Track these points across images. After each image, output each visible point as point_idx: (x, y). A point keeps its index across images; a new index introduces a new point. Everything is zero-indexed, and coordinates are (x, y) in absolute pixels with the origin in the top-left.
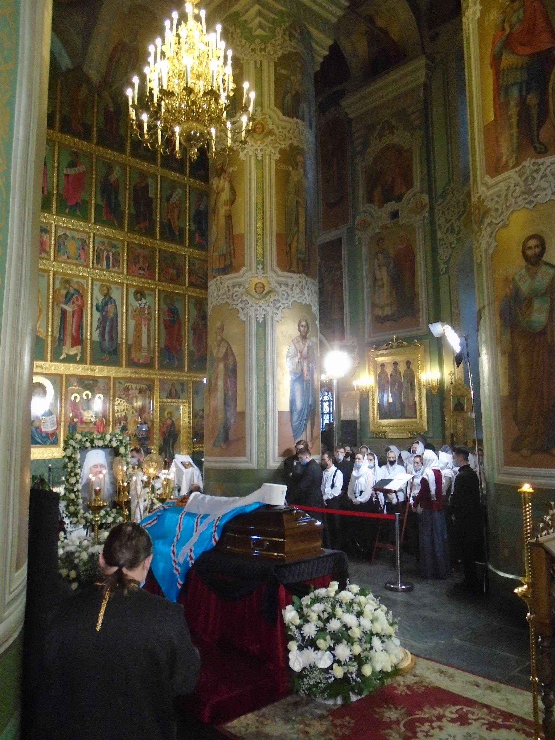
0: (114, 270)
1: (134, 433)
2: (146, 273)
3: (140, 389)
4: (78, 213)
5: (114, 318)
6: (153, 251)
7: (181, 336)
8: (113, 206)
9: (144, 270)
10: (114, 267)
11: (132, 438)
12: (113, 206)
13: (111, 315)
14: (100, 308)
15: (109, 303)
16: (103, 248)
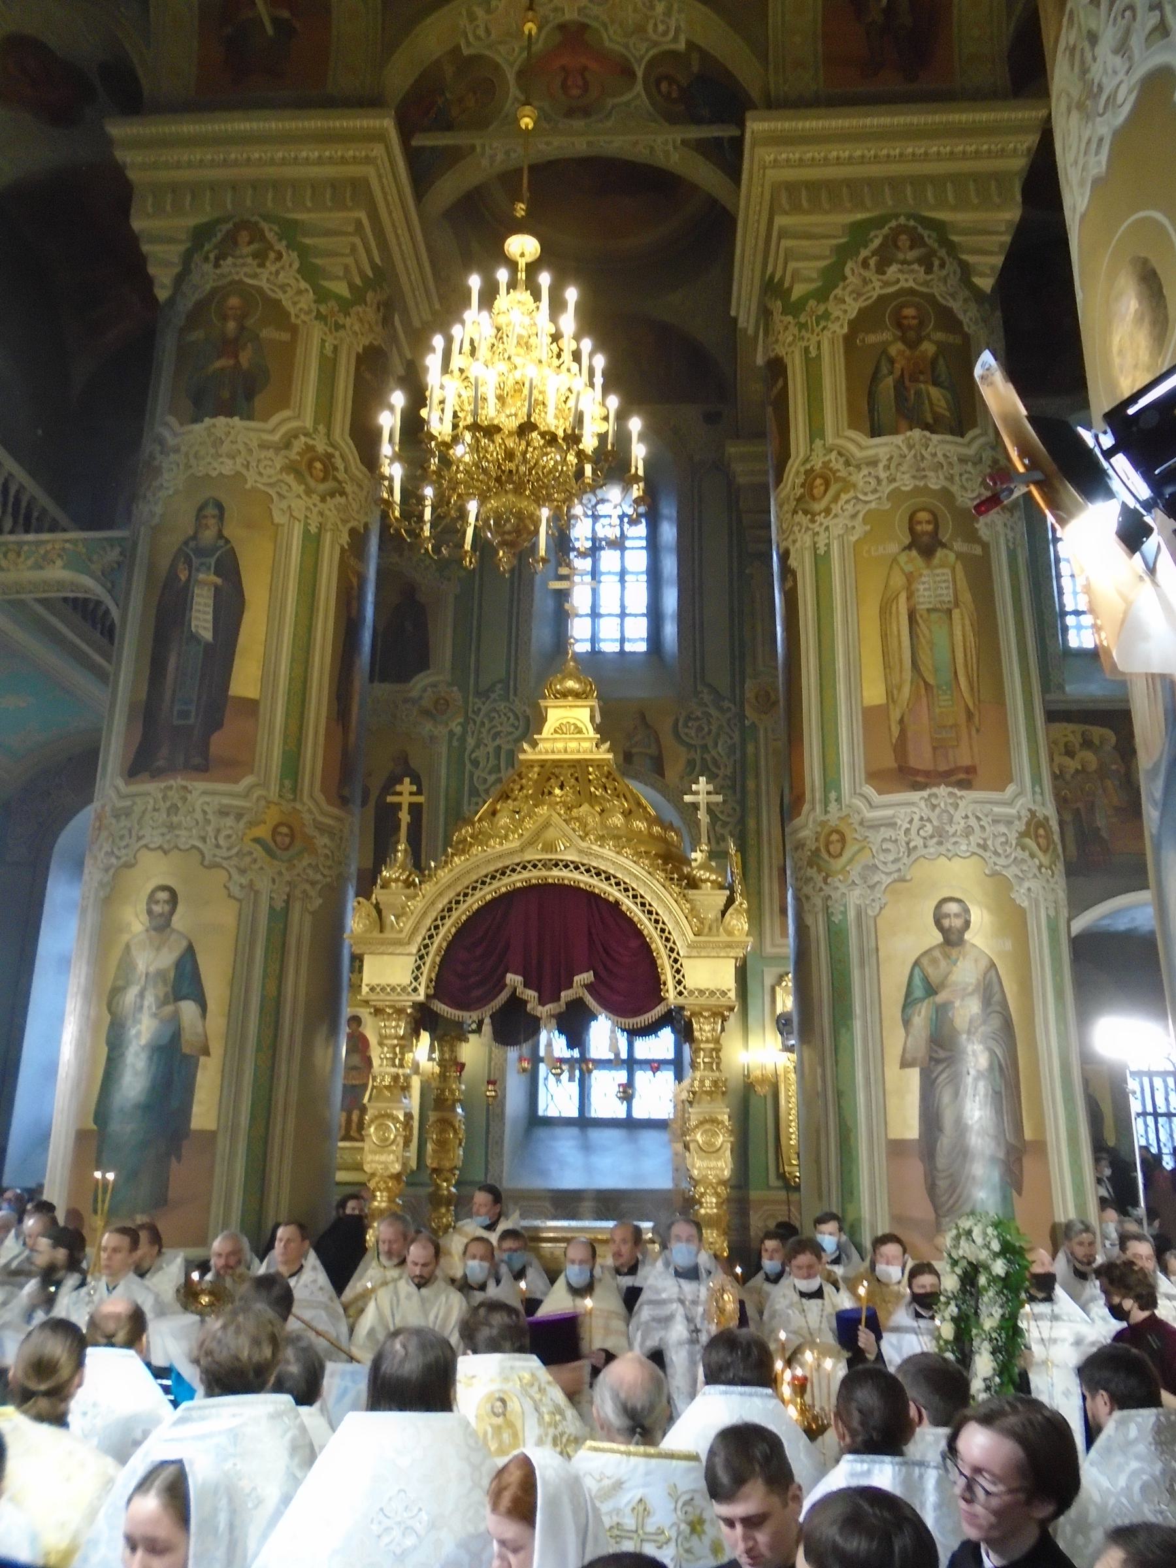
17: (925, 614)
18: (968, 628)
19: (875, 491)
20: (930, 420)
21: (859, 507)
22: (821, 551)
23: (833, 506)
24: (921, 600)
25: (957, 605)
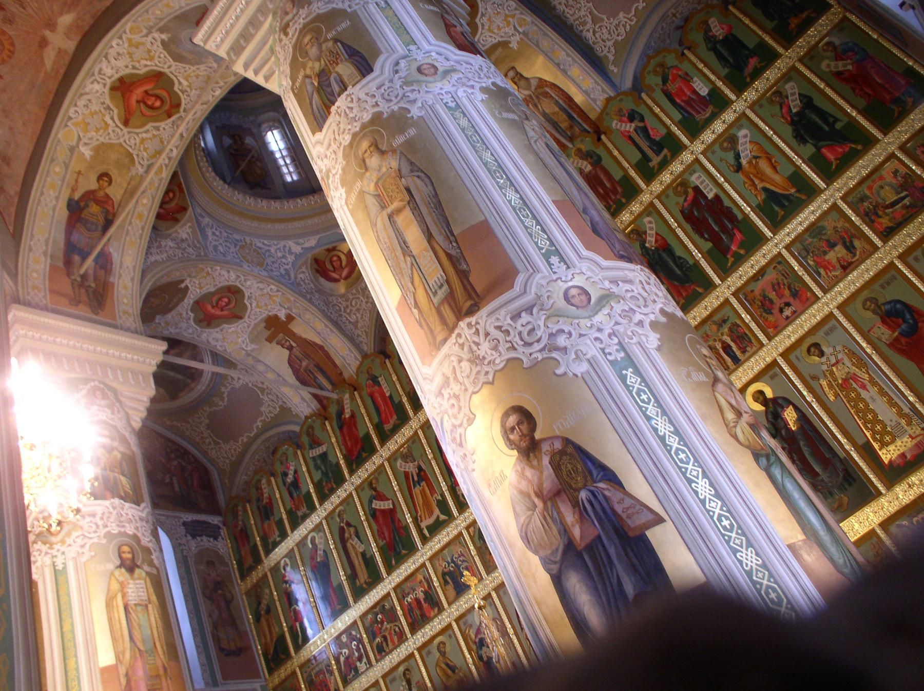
0: (747, 354)
2: (796, 305)
5: (806, 427)
6: (779, 263)
8: (679, 272)
9: (788, 305)
10: (744, 351)
12: (679, 272)
15: (780, 410)
17: (134, 607)
18: (157, 616)
19: (95, 532)
20: (123, 494)
21: (86, 540)
22: (60, 567)
23: (67, 539)
24: (130, 598)
25: (150, 603)
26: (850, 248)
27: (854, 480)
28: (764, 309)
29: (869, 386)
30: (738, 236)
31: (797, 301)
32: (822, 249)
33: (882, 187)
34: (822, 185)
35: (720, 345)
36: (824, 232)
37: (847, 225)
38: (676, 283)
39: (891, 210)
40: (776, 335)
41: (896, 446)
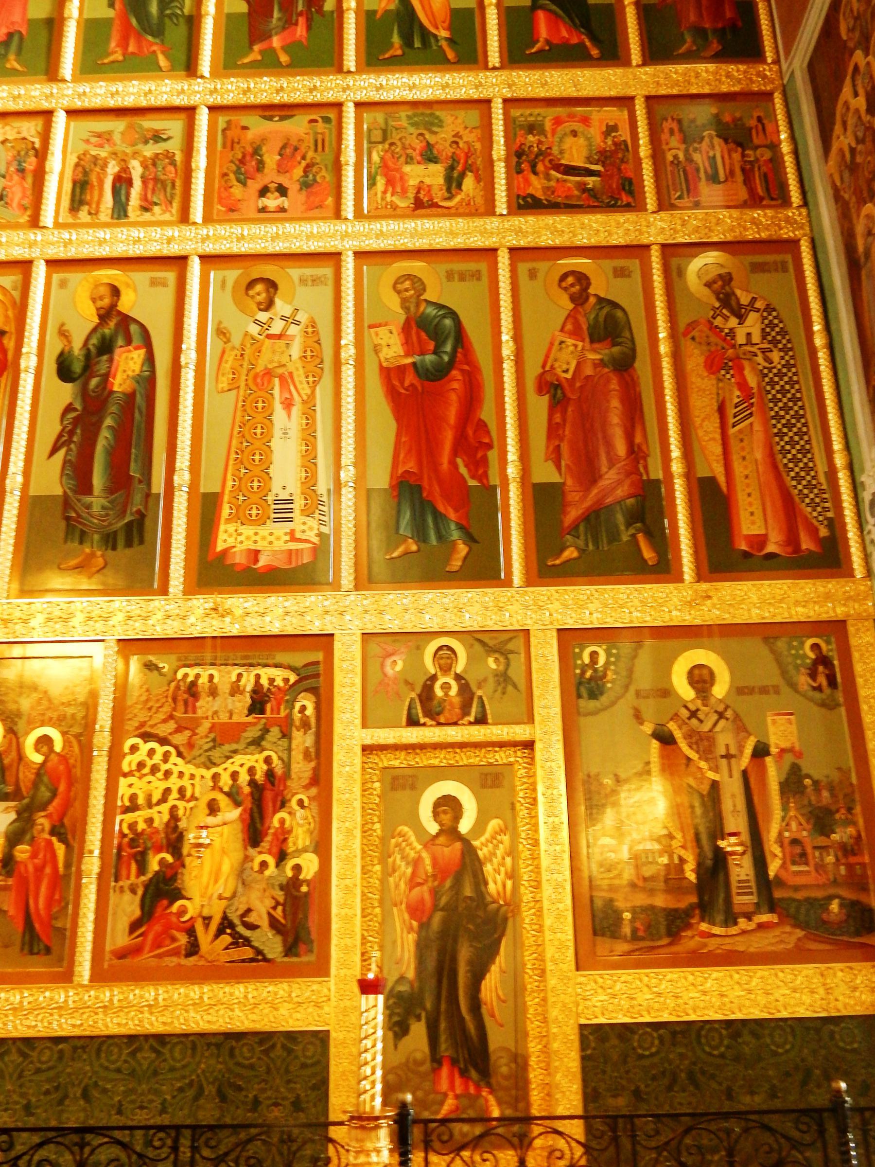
0: (147, 216)
1: (216, 911)
3: (257, 690)
4: (12, 63)
5: (139, 400)
7: (482, 426)
9: (282, 191)
11: (204, 938)
13: (120, 384)
14: (77, 367)
15: (120, 342)
16: (103, 154)
26: (453, 182)
27: (141, 542)
28: (239, 168)
29: (296, 410)
30: (300, 30)
31: (302, 197)
32: (409, 151)
33: (574, 134)
34: (494, 58)
35: (117, 169)
36: (435, 129)
37: (478, 146)
38: (134, 22)
39: (559, 176)
40: (220, 221)
41: (256, 534)
